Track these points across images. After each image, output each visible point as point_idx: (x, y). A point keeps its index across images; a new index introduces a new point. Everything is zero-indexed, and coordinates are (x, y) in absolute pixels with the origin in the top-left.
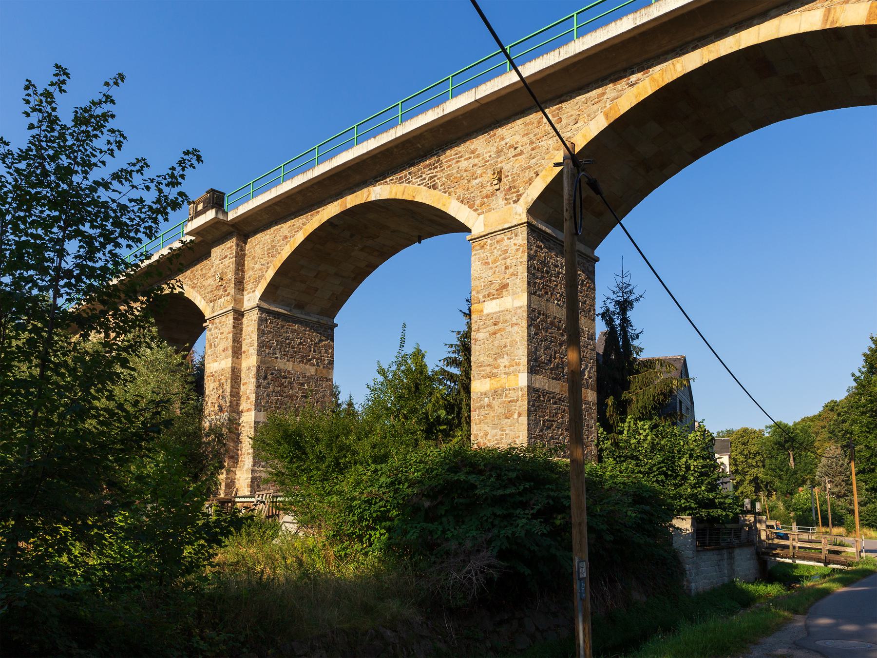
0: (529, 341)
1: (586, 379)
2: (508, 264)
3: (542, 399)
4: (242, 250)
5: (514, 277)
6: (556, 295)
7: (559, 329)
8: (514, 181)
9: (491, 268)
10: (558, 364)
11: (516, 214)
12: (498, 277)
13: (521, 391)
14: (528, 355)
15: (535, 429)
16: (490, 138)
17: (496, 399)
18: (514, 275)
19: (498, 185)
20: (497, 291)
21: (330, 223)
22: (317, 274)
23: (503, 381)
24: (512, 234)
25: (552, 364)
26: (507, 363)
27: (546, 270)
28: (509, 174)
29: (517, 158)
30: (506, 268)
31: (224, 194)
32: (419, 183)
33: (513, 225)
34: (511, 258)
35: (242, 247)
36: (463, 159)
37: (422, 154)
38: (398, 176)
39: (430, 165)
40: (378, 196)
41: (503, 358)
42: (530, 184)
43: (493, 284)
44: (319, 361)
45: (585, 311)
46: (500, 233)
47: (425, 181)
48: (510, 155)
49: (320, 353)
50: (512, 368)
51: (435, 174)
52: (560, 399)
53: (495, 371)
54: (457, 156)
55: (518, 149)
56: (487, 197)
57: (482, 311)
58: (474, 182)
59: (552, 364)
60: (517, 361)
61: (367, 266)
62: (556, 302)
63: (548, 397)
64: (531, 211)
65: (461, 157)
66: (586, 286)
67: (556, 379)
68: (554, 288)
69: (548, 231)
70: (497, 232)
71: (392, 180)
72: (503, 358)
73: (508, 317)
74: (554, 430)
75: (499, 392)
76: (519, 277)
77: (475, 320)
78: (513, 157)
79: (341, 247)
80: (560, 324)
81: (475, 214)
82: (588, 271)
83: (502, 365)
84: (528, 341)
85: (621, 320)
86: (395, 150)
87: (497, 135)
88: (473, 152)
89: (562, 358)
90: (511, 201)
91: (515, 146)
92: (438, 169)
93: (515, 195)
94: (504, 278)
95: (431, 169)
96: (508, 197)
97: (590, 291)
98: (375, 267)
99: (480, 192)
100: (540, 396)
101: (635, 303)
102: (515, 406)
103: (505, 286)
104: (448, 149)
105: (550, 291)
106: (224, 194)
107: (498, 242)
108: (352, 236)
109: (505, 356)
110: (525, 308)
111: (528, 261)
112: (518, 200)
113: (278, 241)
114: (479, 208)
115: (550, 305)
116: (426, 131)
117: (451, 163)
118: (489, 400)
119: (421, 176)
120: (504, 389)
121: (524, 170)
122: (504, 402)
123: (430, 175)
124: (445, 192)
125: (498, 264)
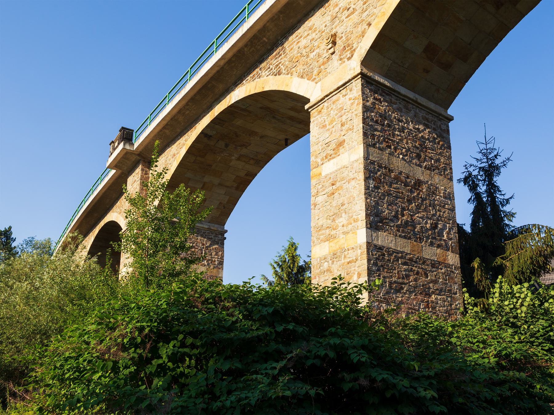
0: (368, 193)
1: (445, 240)
2: (344, 120)
3: (386, 258)
4: (146, 174)
5: (350, 132)
6: (402, 150)
7: (406, 185)
8: (348, 40)
9: (328, 130)
10: (407, 221)
11: (350, 70)
12: (335, 136)
13: (360, 249)
14: (367, 209)
15: (379, 291)
16: (325, 9)
17: (335, 263)
18: (350, 129)
19: (333, 49)
20: (334, 150)
21: (203, 133)
22: (204, 185)
23: (342, 241)
24: (347, 90)
25: (400, 221)
26: (345, 222)
27: (387, 124)
28: (343, 35)
29: (349, 18)
30: (342, 125)
31: (133, 131)
32: (268, 74)
33: (347, 80)
34: (347, 114)
35: (146, 171)
36: (302, 38)
37: (269, 47)
38: (251, 75)
39: (276, 55)
40: (237, 97)
41: (341, 217)
42: (363, 36)
43: (330, 144)
44: (210, 262)
45: (439, 169)
46: (336, 92)
47: (272, 71)
48: (344, 17)
49: (211, 255)
50: (350, 226)
51: (280, 61)
52: (411, 260)
53: (333, 232)
54: (298, 38)
55: (351, 9)
56: (324, 64)
57: (320, 174)
58: (312, 55)
59: (400, 221)
60: (356, 217)
61: (246, 175)
62: (401, 156)
63: (395, 256)
64: (365, 63)
65: (301, 37)
66: (439, 143)
67: (405, 237)
68: (398, 143)
69: (387, 83)
70: (333, 92)
71: (247, 80)
72: (341, 217)
73: (345, 175)
74: (405, 293)
75: (338, 254)
76: (355, 130)
77: (314, 184)
78: (347, 17)
79: (220, 158)
80: (408, 180)
81: (313, 83)
82: (441, 129)
83: (341, 225)
84: (365, 194)
85: (487, 185)
86: (246, 49)
87: (331, 5)
88: (310, 29)
89: (412, 216)
90: (346, 60)
91: (348, 7)
92: (283, 56)
93: (349, 52)
94: (340, 136)
95: (276, 59)
96: (342, 57)
97: (444, 150)
98: (253, 175)
99: (318, 62)
100: (384, 255)
101: (502, 170)
102: (355, 267)
103: (341, 144)
104: (290, 36)
105: (394, 145)
106: (133, 131)
107: (334, 103)
108: (227, 146)
109: (343, 215)
110: (362, 160)
111: (363, 112)
112: (352, 56)
113: (169, 160)
114: (317, 77)
115: (394, 160)
116: (268, 21)
117: (292, 46)
118: (329, 264)
119: (269, 68)
120: (343, 250)
121: (356, 25)
122: (343, 265)
123: (276, 64)
124: (288, 74)
125: (334, 124)
